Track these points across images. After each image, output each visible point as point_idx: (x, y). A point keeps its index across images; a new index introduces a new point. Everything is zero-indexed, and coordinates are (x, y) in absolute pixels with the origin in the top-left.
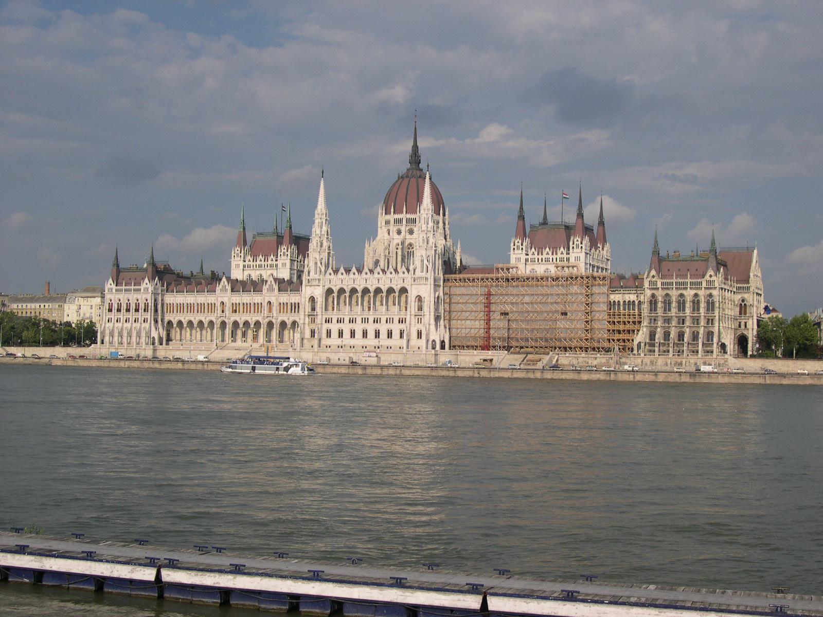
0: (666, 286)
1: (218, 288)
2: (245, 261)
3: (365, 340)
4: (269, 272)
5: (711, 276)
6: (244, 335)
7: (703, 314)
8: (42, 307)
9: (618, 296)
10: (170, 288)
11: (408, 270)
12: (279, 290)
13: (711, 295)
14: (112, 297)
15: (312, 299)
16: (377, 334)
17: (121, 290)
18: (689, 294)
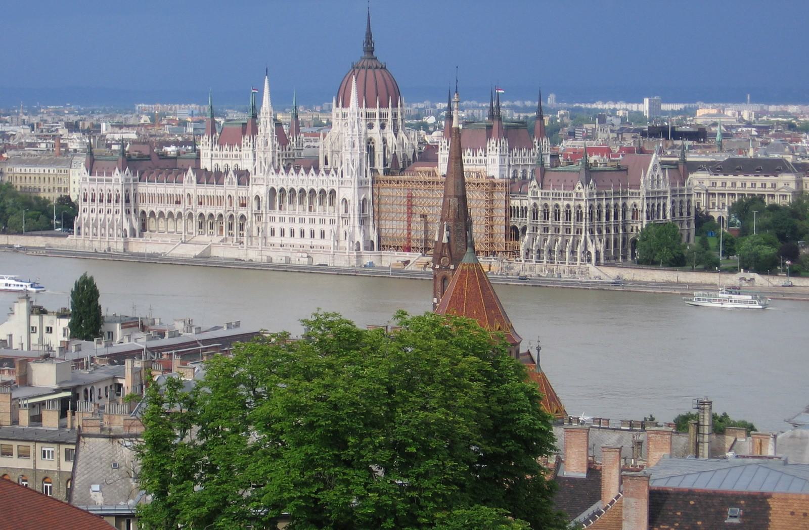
0: (545, 197)
1: (185, 179)
2: (212, 150)
3: (302, 239)
4: (235, 162)
5: (579, 188)
6: (212, 227)
7: (572, 224)
8: (47, 172)
9: (517, 201)
10: (145, 176)
11: (336, 174)
12: (239, 184)
13: (580, 207)
14: (86, 186)
15: (257, 198)
16: (312, 235)
17: (94, 180)
18: (563, 204)
